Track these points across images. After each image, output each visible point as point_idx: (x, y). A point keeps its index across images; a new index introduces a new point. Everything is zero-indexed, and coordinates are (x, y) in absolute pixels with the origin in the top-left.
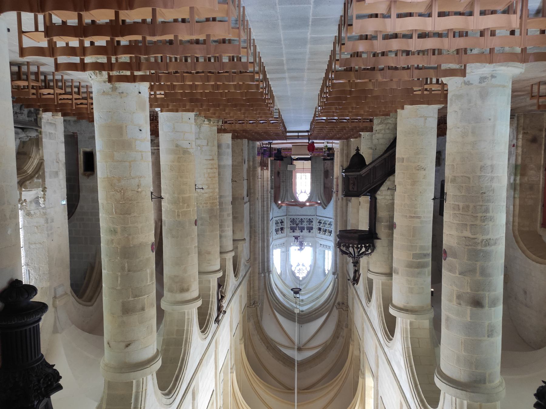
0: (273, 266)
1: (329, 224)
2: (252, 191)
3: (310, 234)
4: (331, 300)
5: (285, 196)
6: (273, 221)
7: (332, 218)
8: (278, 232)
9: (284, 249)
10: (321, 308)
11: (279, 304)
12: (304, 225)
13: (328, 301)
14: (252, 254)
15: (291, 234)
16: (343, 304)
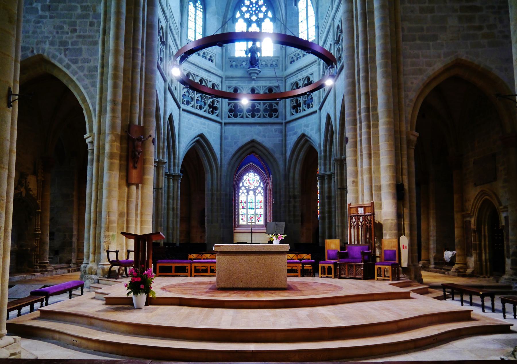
5: (290, 166)
7: (183, 110)
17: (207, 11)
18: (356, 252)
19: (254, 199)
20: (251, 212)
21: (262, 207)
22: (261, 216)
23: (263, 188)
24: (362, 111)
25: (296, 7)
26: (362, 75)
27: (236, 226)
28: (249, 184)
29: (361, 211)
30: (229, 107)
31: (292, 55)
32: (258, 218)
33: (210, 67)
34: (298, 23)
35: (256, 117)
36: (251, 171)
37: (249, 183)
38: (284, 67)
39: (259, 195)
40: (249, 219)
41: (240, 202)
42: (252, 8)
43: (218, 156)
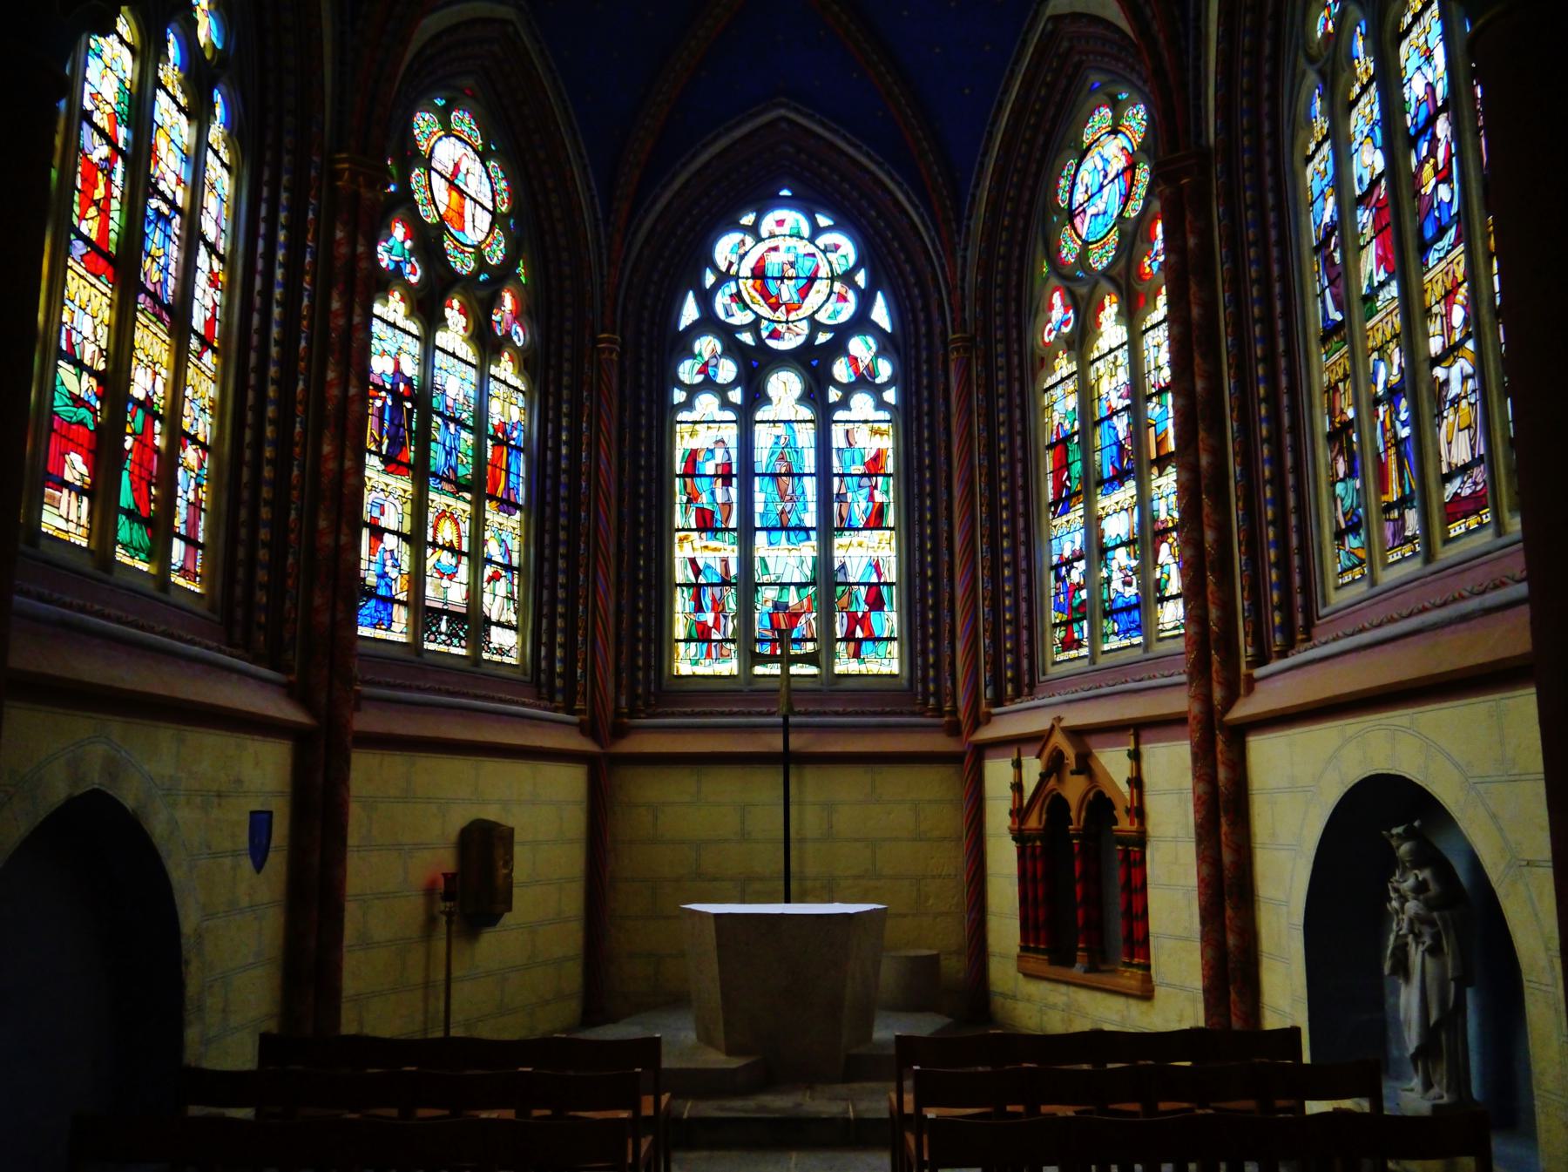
19: (806, 437)
21: (890, 519)
22: (876, 603)
23: (888, 345)
27: (633, 697)
28: (765, 311)
32: (854, 620)
36: (785, 193)
37: (765, 294)
39: (862, 404)
40: (761, 624)
41: (679, 467)
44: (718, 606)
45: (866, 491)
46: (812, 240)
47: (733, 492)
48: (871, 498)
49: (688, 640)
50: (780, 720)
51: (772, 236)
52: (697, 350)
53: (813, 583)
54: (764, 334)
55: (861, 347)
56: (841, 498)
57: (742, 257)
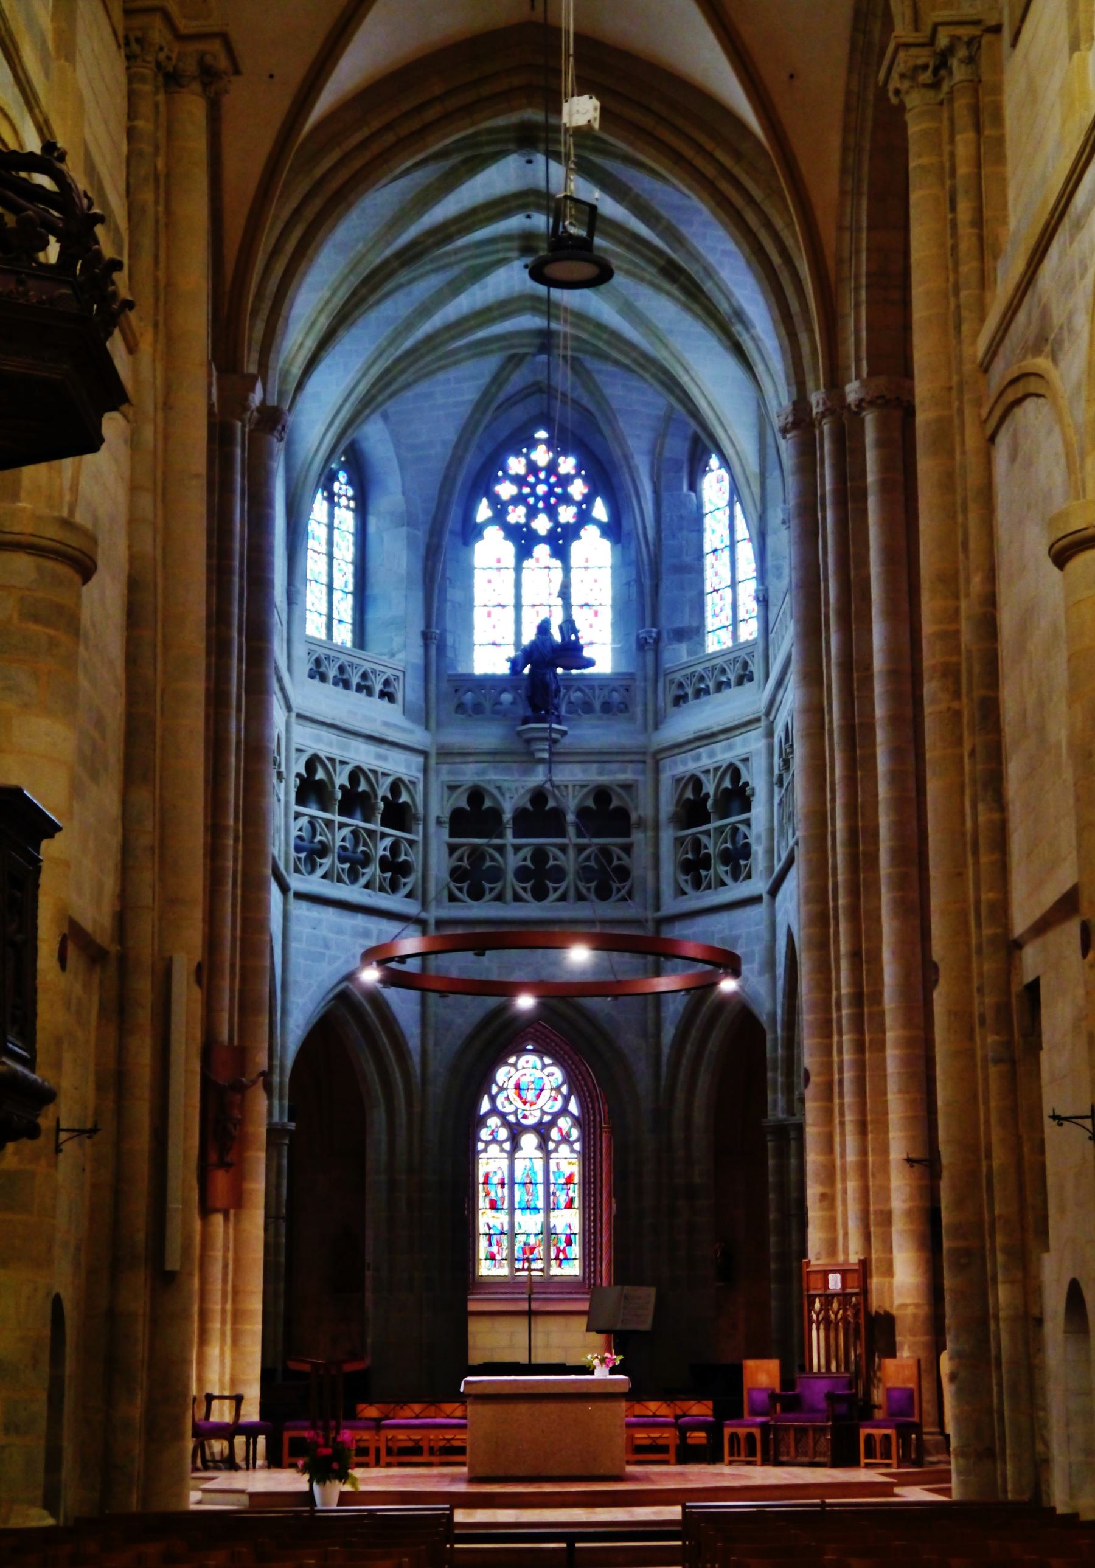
0: (762, 518)
1: (323, 850)
2: (988, 1041)
3: (470, 774)
4: (297, 212)
6: (771, 868)
8: (727, 784)
9: (678, 655)
10: (376, 148)
11: (710, 171)
12: (517, 848)
13: (317, 203)
14: (974, 478)
15: (626, 776)
16: (172, 80)
17: (372, 509)
18: (817, 1392)
19: (539, 1165)
20: (529, 1224)
21: (576, 1204)
22: (569, 1242)
23: (577, 1122)
24: (844, 1002)
25: (693, 494)
26: (841, 901)
28: (519, 1104)
29: (835, 1282)
30: (454, 862)
31: (678, 676)
32: (559, 1250)
33: (386, 724)
34: (700, 556)
35: (553, 896)
36: (530, 1047)
38: (650, 716)
39: (564, 1149)
40: (518, 1253)
41: (481, 1179)
42: (533, 487)
43: (414, 1042)
44: (499, 1244)
45: (565, 1191)
46: (542, 1070)
47: (506, 1190)
48: (567, 1194)
49: (486, 1259)
50: (527, 1296)
51: (523, 1068)
52: (488, 1124)
53: (541, 1233)
54: (520, 1116)
55: (564, 1123)
56: (554, 1194)
57: (509, 1078)
